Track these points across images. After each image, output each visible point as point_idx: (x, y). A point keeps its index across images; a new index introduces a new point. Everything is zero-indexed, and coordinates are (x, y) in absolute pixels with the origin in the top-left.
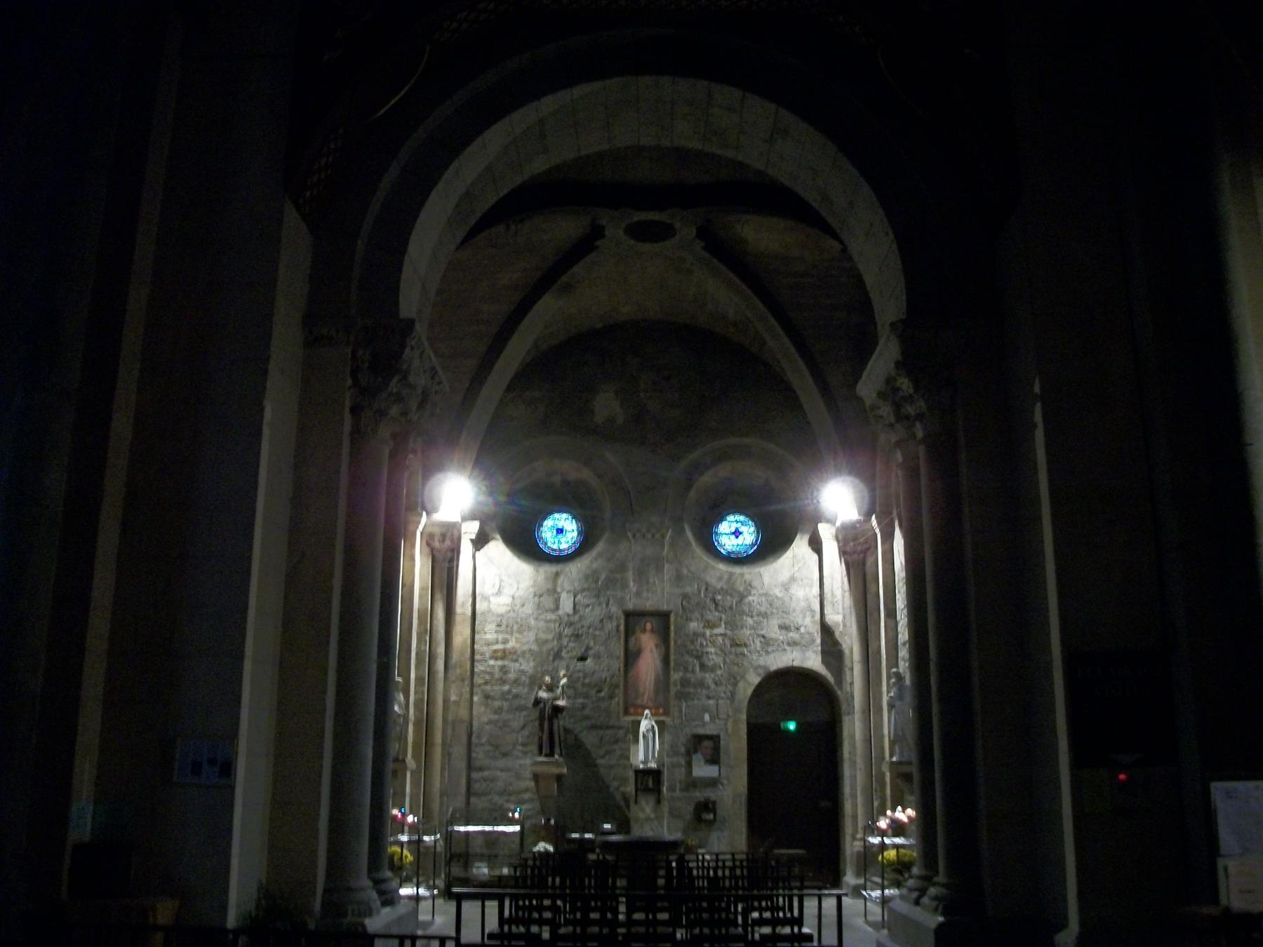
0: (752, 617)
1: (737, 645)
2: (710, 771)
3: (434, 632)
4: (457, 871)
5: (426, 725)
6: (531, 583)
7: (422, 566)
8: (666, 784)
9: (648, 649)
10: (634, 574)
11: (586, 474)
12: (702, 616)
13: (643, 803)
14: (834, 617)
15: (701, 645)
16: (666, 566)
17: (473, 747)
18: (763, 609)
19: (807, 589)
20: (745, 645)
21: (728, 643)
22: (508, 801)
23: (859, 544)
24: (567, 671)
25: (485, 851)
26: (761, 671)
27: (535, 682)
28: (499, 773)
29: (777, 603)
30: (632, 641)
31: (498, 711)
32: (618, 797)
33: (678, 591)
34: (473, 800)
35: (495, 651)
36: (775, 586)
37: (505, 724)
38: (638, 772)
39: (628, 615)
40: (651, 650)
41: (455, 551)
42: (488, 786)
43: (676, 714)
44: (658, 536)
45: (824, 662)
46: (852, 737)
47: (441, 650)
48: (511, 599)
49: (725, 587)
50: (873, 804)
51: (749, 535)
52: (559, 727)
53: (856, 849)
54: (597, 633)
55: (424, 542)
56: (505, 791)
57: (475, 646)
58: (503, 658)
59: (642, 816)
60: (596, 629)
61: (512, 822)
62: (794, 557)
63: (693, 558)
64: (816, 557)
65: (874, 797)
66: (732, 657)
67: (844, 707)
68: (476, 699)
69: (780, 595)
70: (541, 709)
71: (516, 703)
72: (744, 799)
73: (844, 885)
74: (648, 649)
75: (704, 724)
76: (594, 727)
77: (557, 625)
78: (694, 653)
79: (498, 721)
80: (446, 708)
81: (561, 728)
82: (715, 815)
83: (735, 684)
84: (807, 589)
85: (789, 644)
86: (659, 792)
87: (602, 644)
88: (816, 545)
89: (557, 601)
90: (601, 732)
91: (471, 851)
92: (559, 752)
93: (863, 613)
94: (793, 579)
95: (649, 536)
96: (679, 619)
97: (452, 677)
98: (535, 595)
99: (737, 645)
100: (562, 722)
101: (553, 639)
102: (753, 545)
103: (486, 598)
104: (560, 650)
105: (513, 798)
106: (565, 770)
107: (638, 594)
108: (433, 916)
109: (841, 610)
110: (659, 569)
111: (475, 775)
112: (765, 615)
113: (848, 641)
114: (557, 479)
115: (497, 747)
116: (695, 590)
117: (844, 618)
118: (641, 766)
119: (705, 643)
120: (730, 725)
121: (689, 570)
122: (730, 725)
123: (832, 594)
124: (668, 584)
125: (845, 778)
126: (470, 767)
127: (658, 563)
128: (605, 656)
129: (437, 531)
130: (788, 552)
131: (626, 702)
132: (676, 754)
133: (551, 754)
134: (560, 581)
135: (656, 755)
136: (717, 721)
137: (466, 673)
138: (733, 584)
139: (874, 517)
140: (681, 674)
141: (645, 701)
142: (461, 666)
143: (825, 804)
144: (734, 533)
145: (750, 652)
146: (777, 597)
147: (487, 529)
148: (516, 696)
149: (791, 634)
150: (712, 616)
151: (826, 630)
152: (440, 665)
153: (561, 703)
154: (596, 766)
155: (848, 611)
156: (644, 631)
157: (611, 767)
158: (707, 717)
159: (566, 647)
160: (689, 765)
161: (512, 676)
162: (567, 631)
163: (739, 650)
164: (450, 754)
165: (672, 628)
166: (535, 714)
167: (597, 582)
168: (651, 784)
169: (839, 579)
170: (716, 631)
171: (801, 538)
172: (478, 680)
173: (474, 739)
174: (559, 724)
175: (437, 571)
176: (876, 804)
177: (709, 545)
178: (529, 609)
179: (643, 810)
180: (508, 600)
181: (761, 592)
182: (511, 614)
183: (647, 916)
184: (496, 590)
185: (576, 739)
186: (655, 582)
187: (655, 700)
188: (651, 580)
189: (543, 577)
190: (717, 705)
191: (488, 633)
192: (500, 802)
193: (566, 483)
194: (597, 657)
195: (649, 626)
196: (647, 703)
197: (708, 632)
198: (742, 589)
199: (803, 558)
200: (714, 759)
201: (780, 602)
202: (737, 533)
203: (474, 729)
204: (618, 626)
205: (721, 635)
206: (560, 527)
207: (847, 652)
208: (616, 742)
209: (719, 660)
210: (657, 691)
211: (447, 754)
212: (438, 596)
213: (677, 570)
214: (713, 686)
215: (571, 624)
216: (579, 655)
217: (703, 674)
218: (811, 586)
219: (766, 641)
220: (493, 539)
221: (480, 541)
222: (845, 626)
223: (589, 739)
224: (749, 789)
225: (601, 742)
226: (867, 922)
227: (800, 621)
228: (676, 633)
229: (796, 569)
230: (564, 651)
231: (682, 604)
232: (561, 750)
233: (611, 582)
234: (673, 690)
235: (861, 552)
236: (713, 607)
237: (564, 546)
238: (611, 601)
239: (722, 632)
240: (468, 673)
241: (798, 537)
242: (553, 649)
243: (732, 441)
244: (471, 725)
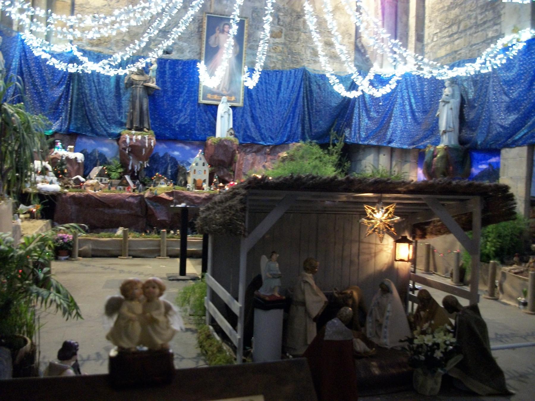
30: (212, 38)
138: (293, 5)
196: (222, 91)
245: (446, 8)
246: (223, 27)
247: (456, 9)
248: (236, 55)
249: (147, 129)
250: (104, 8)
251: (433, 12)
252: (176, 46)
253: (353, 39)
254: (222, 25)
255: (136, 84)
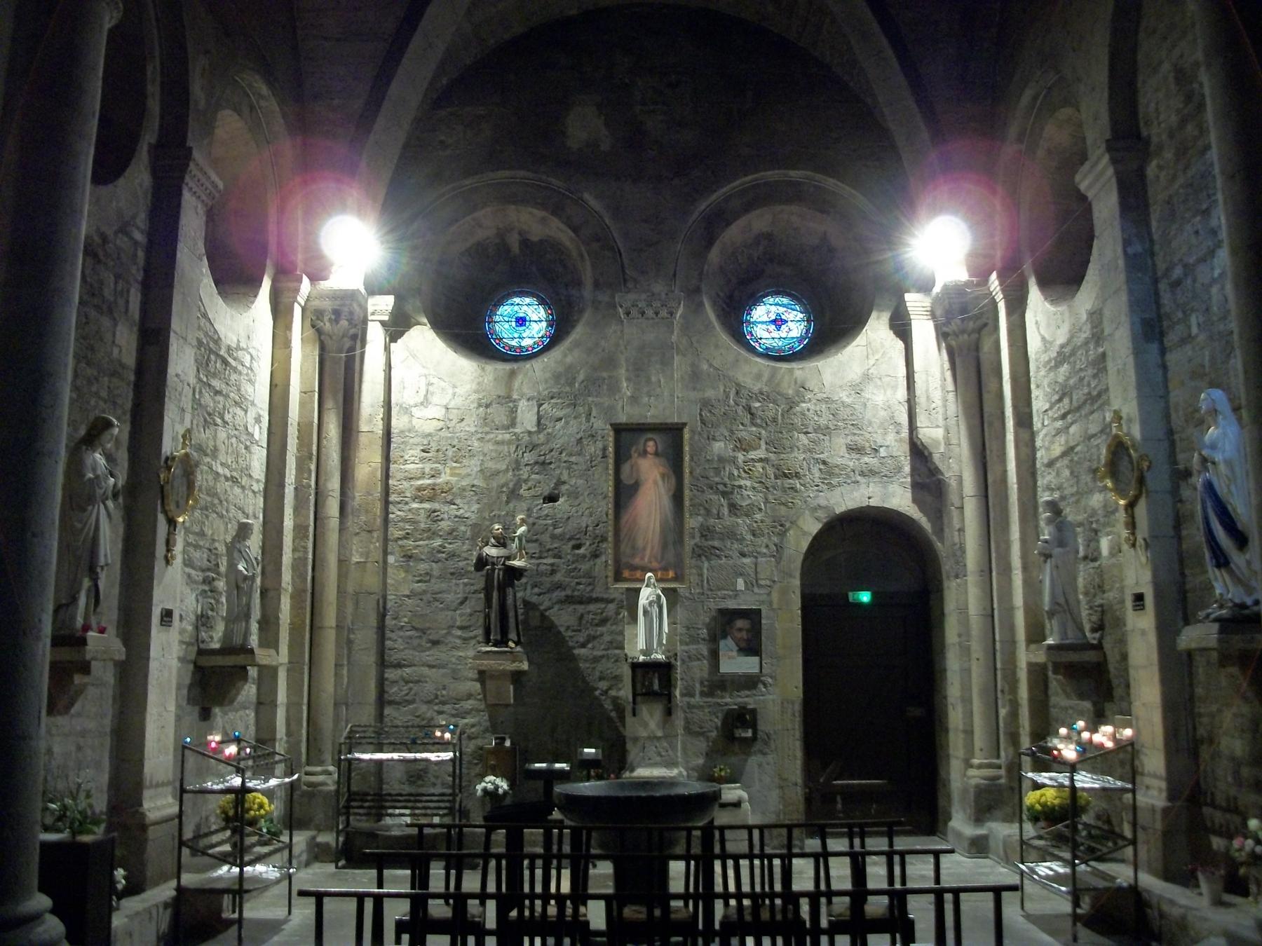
0: (806, 433)
1: (785, 475)
2: (748, 665)
3: (323, 458)
4: (360, 822)
5: (311, 599)
6: (474, 386)
7: (305, 357)
8: (679, 683)
9: (650, 481)
10: (627, 370)
11: (557, 230)
12: (732, 432)
13: (644, 710)
14: (931, 432)
15: (731, 475)
16: (677, 359)
17: (388, 634)
18: (823, 422)
19: (889, 392)
20: (797, 475)
21: (771, 471)
22: (440, 713)
23: (970, 318)
24: (529, 516)
25: (407, 789)
26: (821, 514)
27: (479, 533)
28: (426, 670)
29: (844, 413)
30: (626, 468)
31: (426, 577)
32: (608, 705)
33: (693, 395)
34: (387, 711)
35: (419, 489)
36: (841, 387)
37: (436, 597)
38: (636, 666)
39: (619, 429)
40: (655, 483)
41: (359, 338)
42: (411, 689)
43: (694, 579)
44: (664, 313)
45: (915, 501)
46: (963, 611)
47: (334, 484)
48: (444, 410)
49: (765, 389)
50: (997, 712)
51: (796, 326)
52: (515, 601)
53: (974, 782)
54: (573, 459)
55: (308, 323)
56: (437, 697)
57: (391, 482)
58: (430, 500)
59: (643, 733)
60: (571, 455)
61: (442, 745)
62: (868, 344)
63: (717, 346)
64: (900, 345)
65: (1000, 702)
66: (778, 493)
67: (947, 566)
68: (391, 559)
69: (848, 400)
70: (488, 574)
71: (452, 565)
72: (798, 707)
73: (950, 837)
74: (650, 481)
75: (737, 594)
76: (569, 600)
77: (513, 448)
78: (721, 487)
79: (425, 592)
80: (343, 575)
81: (520, 604)
82: (755, 733)
83: (782, 534)
84: (889, 392)
85: (862, 474)
86: (669, 697)
87: (580, 477)
88: (901, 328)
89: (513, 411)
90: (581, 609)
91: (386, 788)
92: (516, 639)
93: (977, 422)
94: (867, 377)
95: (650, 313)
96: (696, 437)
97: (352, 524)
98: (480, 406)
99: (785, 475)
100: (522, 592)
101: (507, 470)
102: (801, 340)
103: (406, 410)
104: (518, 485)
105: (446, 708)
106: (525, 666)
107: (634, 399)
108: (290, 913)
109: (941, 422)
110: (666, 363)
111: (391, 674)
112: (826, 431)
113: (955, 466)
114: (514, 241)
115: (423, 631)
116: (721, 395)
117: (947, 431)
118: (642, 658)
119: (736, 473)
120: (775, 596)
121: (711, 365)
122: (775, 596)
123: (928, 397)
124: (680, 385)
125: (949, 674)
126: (382, 664)
127: (664, 354)
128: (586, 493)
129: (327, 305)
130: (859, 338)
131: (617, 561)
132: (694, 640)
133: (503, 642)
134: (516, 384)
135: (664, 642)
136: (756, 590)
137: (375, 519)
138: (778, 384)
139: (994, 276)
140: (700, 519)
141: (646, 560)
142: (367, 512)
143: (915, 712)
144: (774, 322)
145: (803, 485)
146: (843, 402)
147: (409, 308)
148: (452, 555)
149: (866, 459)
150: (746, 432)
151: (919, 452)
152: (332, 507)
153: (517, 563)
154: (574, 658)
155: (952, 422)
156: (644, 453)
157: (596, 660)
158: (741, 585)
159: (526, 481)
160: (715, 655)
161: (445, 525)
162: (529, 457)
163: (788, 482)
164: (350, 642)
165: (687, 448)
166: (480, 583)
167: (571, 384)
168: (656, 687)
169: (938, 375)
170: (753, 455)
171: (878, 318)
172: (395, 532)
173: (389, 621)
174: (515, 596)
175: (328, 365)
176: (1003, 712)
177: (737, 329)
178: (470, 425)
179: (646, 725)
180: (439, 413)
181: (820, 396)
182: (444, 433)
183: (650, 913)
184: (420, 398)
185: (543, 617)
186: (660, 381)
187: (662, 558)
188: (654, 379)
189: (491, 378)
190: (756, 565)
191: (409, 462)
192: (429, 715)
193: (525, 243)
194: (574, 494)
195: (651, 446)
197: (741, 457)
198: (790, 392)
199: (882, 346)
200: (752, 647)
201: (848, 411)
202: (778, 322)
203: (389, 604)
204: (605, 449)
205: (761, 460)
206: (522, 315)
207: (953, 483)
208: (604, 622)
209: (758, 498)
210: (664, 546)
211: (346, 644)
212: (329, 404)
213: (693, 365)
214: (749, 537)
215: (533, 447)
216: (546, 490)
217: (733, 519)
218: (895, 388)
219: (829, 471)
220: (419, 323)
221: (397, 327)
222: (948, 444)
223: (563, 618)
224: (805, 692)
225: (580, 624)
226: (1028, 917)
227: (880, 441)
228: (692, 459)
229: (872, 362)
230: (524, 487)
231: (701, 415)
232: (518, 635)
233: (593, 384)
234: (689, 543)
235: (973, 331)
236: (747, 421)
237: (527, 343)
238: (594, 413)
239: (763, 456)
240: (379, 521)
241: (874, 315)
242: (506, 484)
243: (772, 175)
244: (385, 598)
245: (1053, 364)
246: (645, 444)
247: (1065, 365)
248: (671, 493)
249: (514, 642)
250: (440, 433)
251: (1038, 368)
252: (564, 488)
253: (905, 433)
254: (642, 441)
255: (493, 564)
